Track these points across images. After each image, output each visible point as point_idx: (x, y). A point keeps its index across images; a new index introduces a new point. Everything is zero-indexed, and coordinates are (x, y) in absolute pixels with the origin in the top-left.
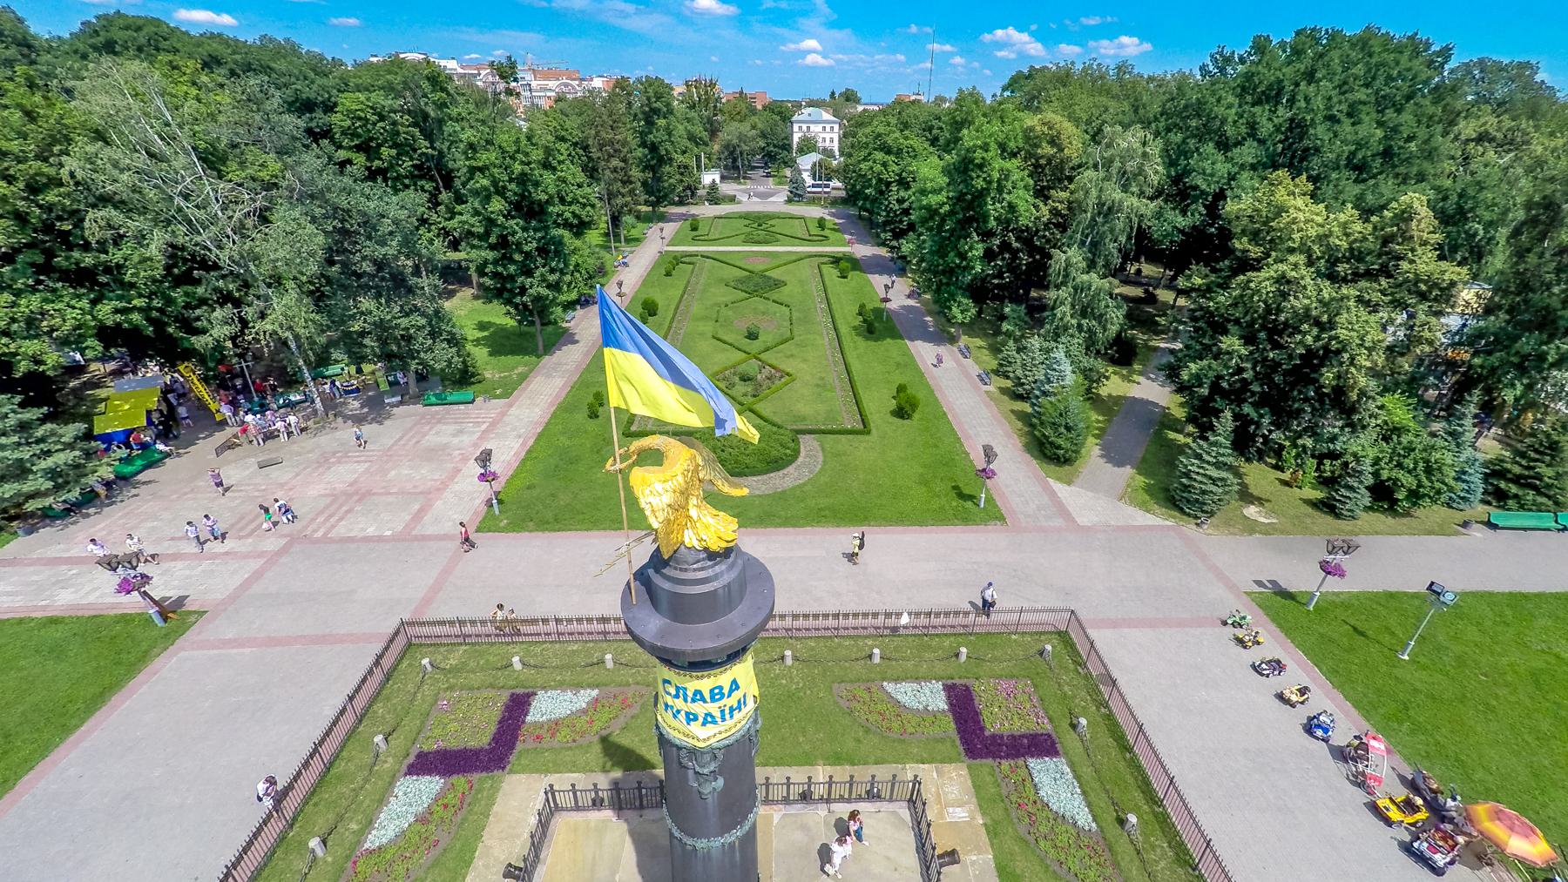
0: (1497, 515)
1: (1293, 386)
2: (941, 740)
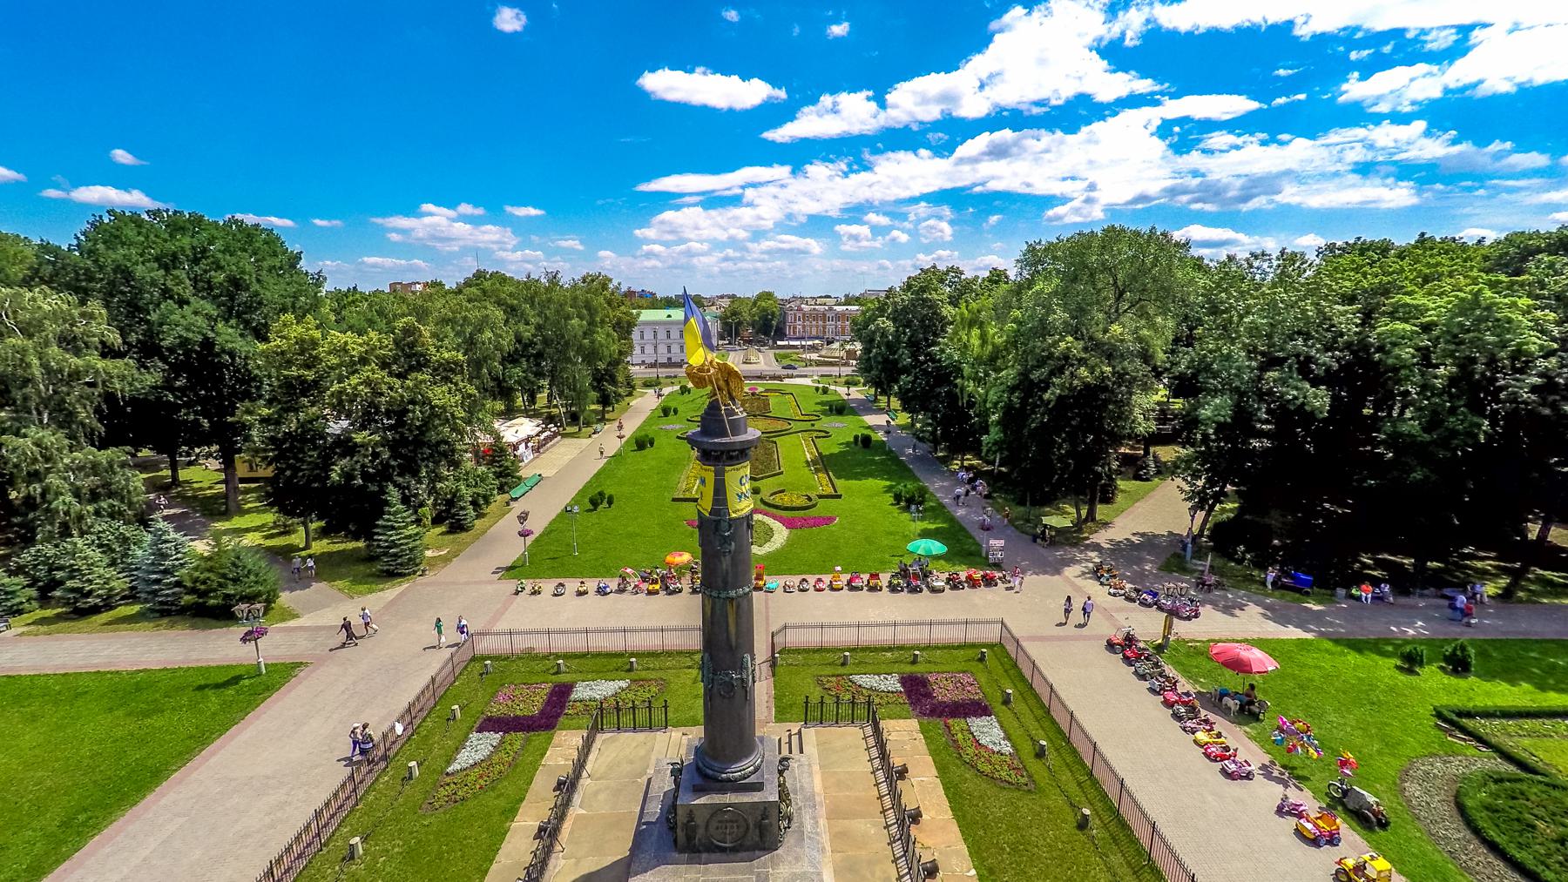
0: (515, 493)
1: (414, 451)
2: (527, 740)
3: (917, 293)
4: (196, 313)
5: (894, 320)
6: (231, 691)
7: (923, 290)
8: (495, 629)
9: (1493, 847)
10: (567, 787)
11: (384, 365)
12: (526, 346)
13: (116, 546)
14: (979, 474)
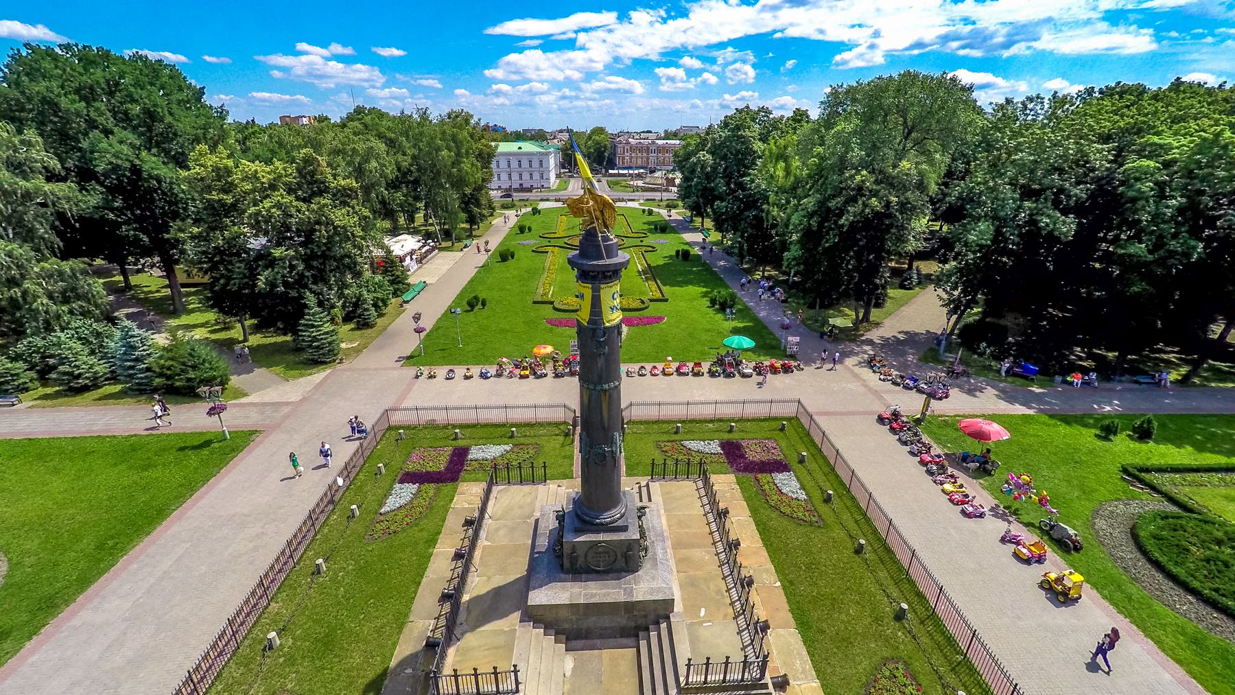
0: (406, 297)
1: (324, 263)
2: (438, 489)
3: (732, 130)
4: (121, 142)
5: (713, 153)
6: (205, 452)
7: (738, 128)
8: (403, 406)
9: (1157, 565)
10: (473, 524)
11: (290, 191)
12: (405, 174)
13: (92, 339)
14: (778, 283)
